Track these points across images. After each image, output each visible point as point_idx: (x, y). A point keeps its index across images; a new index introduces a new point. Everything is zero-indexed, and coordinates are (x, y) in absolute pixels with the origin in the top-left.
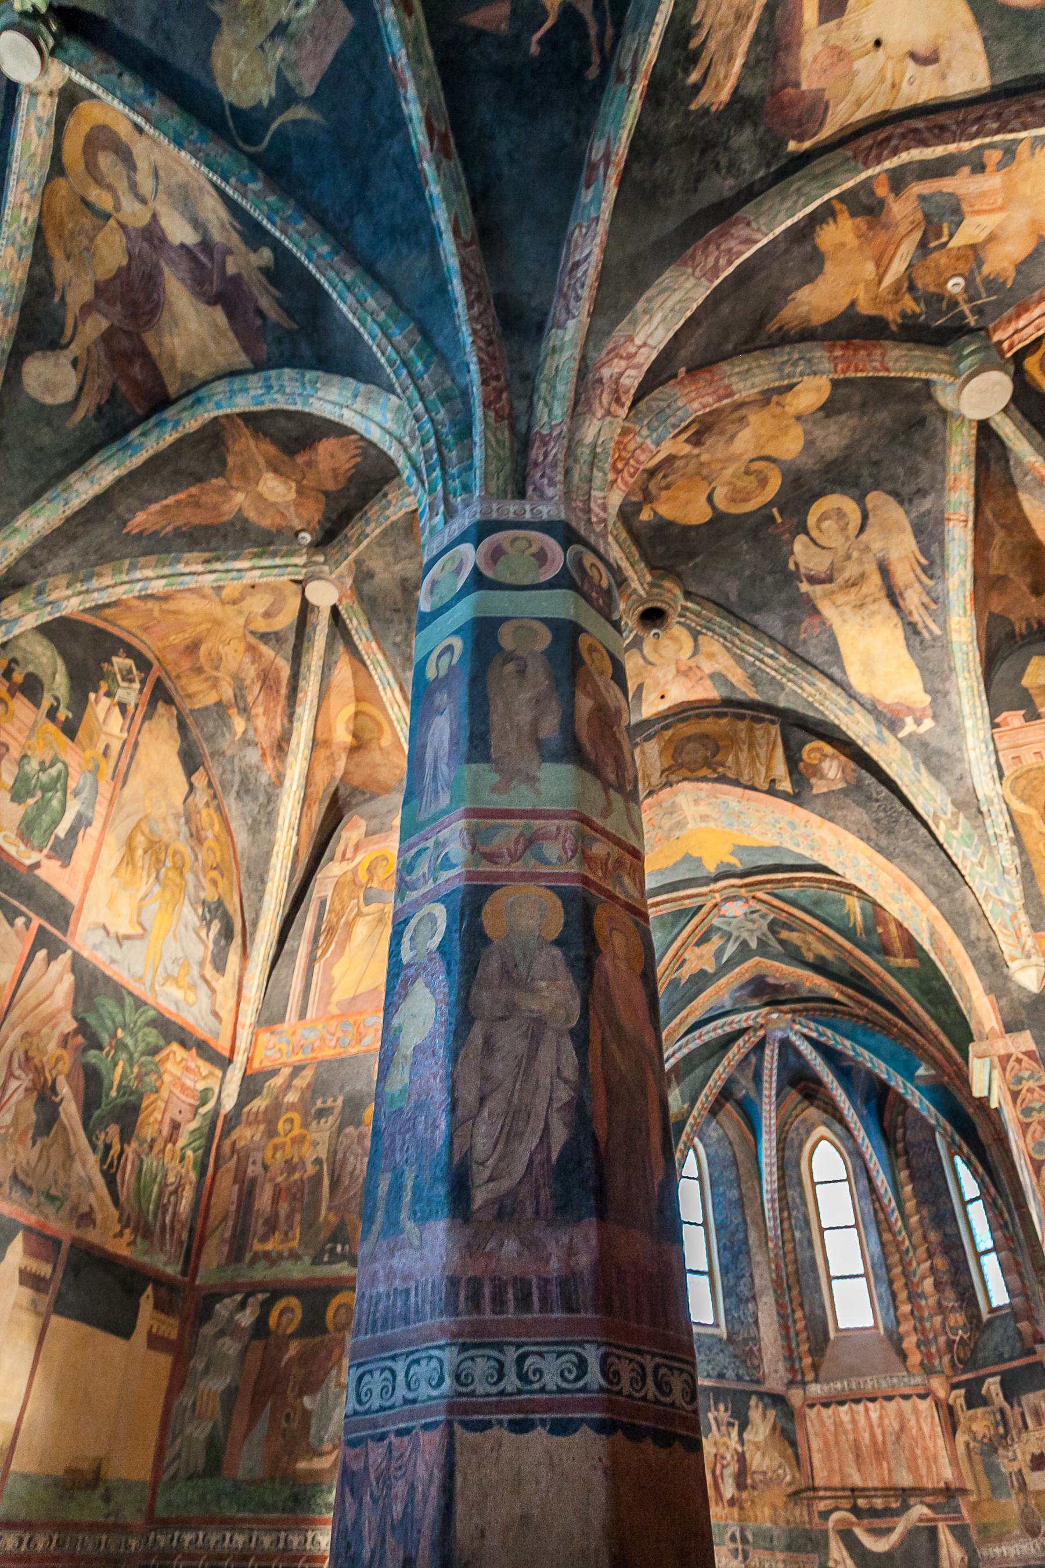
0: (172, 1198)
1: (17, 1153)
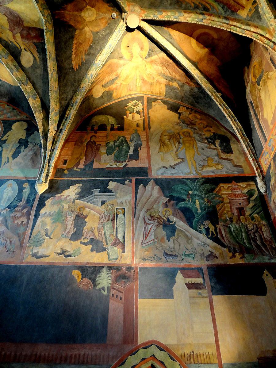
0: (256, 234)
1: (162, 246)
